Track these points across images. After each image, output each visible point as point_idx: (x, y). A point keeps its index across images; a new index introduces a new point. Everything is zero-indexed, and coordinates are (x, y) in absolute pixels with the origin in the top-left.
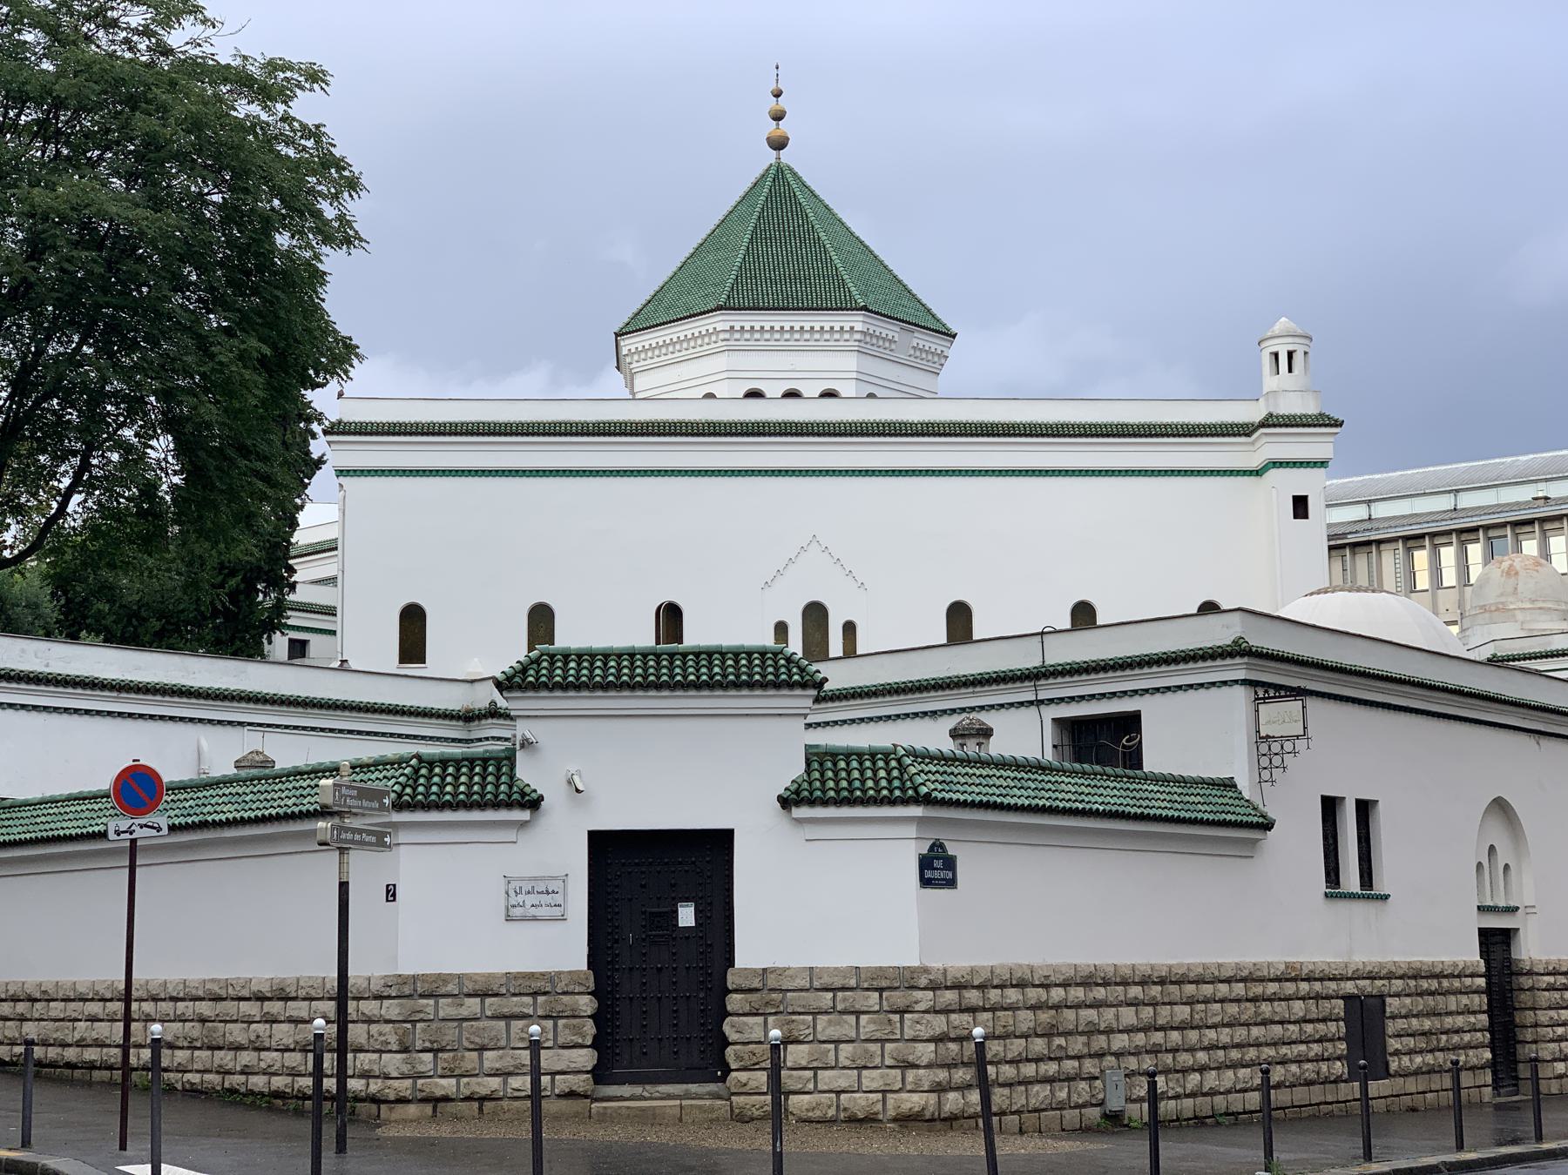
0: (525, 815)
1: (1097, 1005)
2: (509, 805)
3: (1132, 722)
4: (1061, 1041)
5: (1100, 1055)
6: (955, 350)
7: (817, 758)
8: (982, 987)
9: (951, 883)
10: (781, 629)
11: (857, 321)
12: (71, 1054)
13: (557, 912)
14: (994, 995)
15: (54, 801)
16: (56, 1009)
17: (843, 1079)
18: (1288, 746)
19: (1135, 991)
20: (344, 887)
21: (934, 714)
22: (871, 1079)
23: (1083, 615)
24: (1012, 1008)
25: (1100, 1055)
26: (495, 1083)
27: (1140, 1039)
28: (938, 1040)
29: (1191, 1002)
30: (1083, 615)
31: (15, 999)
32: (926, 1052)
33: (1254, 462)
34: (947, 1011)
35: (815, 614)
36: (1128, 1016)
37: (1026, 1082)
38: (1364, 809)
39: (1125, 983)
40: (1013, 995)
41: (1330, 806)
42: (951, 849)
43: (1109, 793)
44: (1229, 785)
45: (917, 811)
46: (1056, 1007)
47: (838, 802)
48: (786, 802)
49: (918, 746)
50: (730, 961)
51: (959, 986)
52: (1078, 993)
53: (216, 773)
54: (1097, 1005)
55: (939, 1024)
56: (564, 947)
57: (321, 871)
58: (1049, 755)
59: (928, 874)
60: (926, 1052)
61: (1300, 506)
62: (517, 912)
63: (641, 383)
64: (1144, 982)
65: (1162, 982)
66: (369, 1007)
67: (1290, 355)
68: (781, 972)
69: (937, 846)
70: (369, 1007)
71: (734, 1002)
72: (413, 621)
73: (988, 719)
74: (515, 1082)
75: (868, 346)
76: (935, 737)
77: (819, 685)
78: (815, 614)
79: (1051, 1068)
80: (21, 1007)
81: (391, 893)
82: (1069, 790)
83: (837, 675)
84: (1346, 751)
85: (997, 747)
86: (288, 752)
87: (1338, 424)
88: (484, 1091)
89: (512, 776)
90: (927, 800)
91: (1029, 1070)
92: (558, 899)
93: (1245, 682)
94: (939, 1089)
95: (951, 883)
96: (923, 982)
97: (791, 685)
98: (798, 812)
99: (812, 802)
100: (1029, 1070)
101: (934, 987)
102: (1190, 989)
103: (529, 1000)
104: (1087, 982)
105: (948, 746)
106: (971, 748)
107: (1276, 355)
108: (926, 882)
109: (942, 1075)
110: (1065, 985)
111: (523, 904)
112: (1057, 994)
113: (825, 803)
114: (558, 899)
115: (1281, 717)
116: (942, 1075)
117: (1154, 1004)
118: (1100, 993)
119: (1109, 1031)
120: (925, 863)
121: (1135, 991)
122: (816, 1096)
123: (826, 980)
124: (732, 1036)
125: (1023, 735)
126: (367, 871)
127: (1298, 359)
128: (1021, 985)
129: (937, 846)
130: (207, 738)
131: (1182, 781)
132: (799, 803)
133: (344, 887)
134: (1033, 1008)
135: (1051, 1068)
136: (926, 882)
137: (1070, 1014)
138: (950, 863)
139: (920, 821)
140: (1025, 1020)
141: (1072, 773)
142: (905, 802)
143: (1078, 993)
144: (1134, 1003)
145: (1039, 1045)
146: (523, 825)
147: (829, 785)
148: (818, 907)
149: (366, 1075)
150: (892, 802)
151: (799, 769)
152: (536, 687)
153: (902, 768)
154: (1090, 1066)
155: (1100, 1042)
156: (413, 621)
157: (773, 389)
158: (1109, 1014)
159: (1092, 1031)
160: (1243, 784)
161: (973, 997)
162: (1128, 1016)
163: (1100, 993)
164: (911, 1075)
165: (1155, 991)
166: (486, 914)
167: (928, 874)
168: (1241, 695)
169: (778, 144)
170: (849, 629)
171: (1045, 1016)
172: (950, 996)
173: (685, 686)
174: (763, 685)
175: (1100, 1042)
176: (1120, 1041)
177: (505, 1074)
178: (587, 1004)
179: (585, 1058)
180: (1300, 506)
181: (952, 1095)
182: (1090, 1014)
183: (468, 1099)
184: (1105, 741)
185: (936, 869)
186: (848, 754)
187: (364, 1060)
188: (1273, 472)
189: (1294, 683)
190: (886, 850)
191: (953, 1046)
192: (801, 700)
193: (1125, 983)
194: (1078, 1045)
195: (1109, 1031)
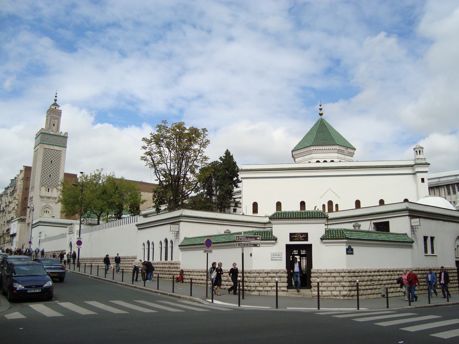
0: (274, 242)
1: (380, 275)
2: (271, 240)
3: (388, 223)
4: (373, 282)
5: (381, 285)
6: (356, 152)
7: (327, 231)
8: (358, 272)
9: (352, 254)
10: (324, 206)
11: (337, 147)
12: (198, 281)
13: (280, 259)
14: (360, 274)
15: (194, 238)
16: (195, 273)
17: (333, 289)
18: (417, 227)
19: (387, 273)
20: (243, 254)
21: (351, 222)
22: (337, 289)
23: (382, 202)
24: (364, 276)
25: (381, 285)
26: (269, 289)
27: (388, 282)
28: (350, 282)
29: (398, 275)
30: (382, 202)
31: (188, 272)
32: (347, 284)
33: (414, 172)
34: (351, 277)
35: (330, 203)
36: (386, 277)
37: (367, 289)
38: (432, 238)
39: (386, 271)
40: (364, 274)
41: (425, 238)
42: (352, 247)
43: (383, 236)
44: (406, 234)
45: (346, 241)
46: (373, 276)
47: (331, 239)
48: (322, 239)
49: (346, 228)
50: (312, 268)
51: (354, 272)
52: (377, 273)
53: (221, 234)
54: (380, 275)
55: (350, 279)
56: (282, 265)
57: (238, 251)
58: (373, 230)
59: (348, 252)
60: (347, 284)
61: (423, 180)
62: (273, 259)
63: (296, 160)
64: (389, 271)
65: (393, 271)
66: (248, 275)
67: (420, 151)
68: (321, 270)
69: (350, 246)
70: (248, 275)
71: (312, 275)
72: (255, 205)
73: (360, 223)
74: (273, 288)
75: (339, 152)
76: (350, 226)
77: (327, 218)
78: (330, 203)
79: (371, 287)
80: (189, 273)
81: (251, 255)
82: (374, 236)
83: (331, 215)
84: (427, 227)
85: (362, 228)
86: (234, 230)
87: (429, 164)
88: (268, 290)
89: (272, 235)
90: (347, 239)
91: (367, 287)
92: (281, 256)
93: (409, 215)
94: (350, 291)
95: (352, 254)
96: (347, 272)
97: (322, 218)
98: (323, 241)
99: (326, 239)
100: (367, 287)
101: (349, 272)
102: (398, 272)
103: (275, 274)
104: (378, 271)
105: (352, 228)
106: (357, 228)
107: (417, 151)
108: (347, 253)
109: (350, 288)
110: (374, 272)
111: (274, 257)
112: (373, 274)
113: (329, 239)
114: (281, 256)
115: (415, 221)
116: (350, 288)
117: (391, 275)
118: (381, 273)
119: (382, 280)
120: (347, 250)
121: (387, 273)
122: (328, 292)
123: (329, 271)
124: (312, 281)
125: (366, 226)
126: (247, 250)
127: (421, 152)
128: (366, 272)
129: (350, 246)
130: (219, 227)
131: (396, 234)
132: (324, 239)
133: (243, 254)
134: (368, 276)
135: (371, 287)
136: (347, 253)
137: (375, 277)
138: (352, 250)
139: (346, 242)
140: (366, 278)
141: (377, 233)
142: (343, 239)
143: (377, 273)
144: (388, 275)
145: (369, 283)
146: (274, 243)
147: (330, 237)
148: (328, 258)
149: (247, 286)
150: (341, 239)
151: (324, 233)
152: (276, 219)
153: (343, 233)
154: (379, 287)
155: (381, 282)
156: (255, 205)
157: (322, 161)
158: (382, 277)
159: (379, 280)
160: (409, 235)
161: (356, 274)
162: (386, 277)
163: (381, 273)
164: (345, 288)
165: (391, 273)
166: (267, 259)
167: (348, 252)
168: (407, 218)
169: (321, 115)
170: (337, 206)
171: (371, 278)
172: (352, 274)
173: (303, 218)
174: (317, 218)
175: (381, 282)
176: (385, 282)
177: (271, 287)
178: (286, 275)
179: (286, 284)
180: (423, 180)
181: (353, 292)
182: (379, 277)
183: (265, 291)
184: (383, 227)
185: (350, 251)
186: (333, 230)
187: (247, 284)
188: (418, 174)
189: (418, 215)
190: (340, 249)
191: (353, 283)
192: (324, 221)
193: (386, 271)
194: (376, 283)
195: (382, 280)
